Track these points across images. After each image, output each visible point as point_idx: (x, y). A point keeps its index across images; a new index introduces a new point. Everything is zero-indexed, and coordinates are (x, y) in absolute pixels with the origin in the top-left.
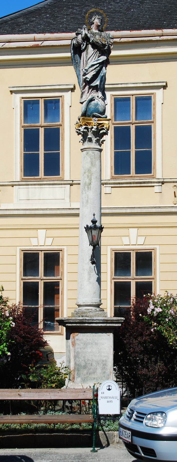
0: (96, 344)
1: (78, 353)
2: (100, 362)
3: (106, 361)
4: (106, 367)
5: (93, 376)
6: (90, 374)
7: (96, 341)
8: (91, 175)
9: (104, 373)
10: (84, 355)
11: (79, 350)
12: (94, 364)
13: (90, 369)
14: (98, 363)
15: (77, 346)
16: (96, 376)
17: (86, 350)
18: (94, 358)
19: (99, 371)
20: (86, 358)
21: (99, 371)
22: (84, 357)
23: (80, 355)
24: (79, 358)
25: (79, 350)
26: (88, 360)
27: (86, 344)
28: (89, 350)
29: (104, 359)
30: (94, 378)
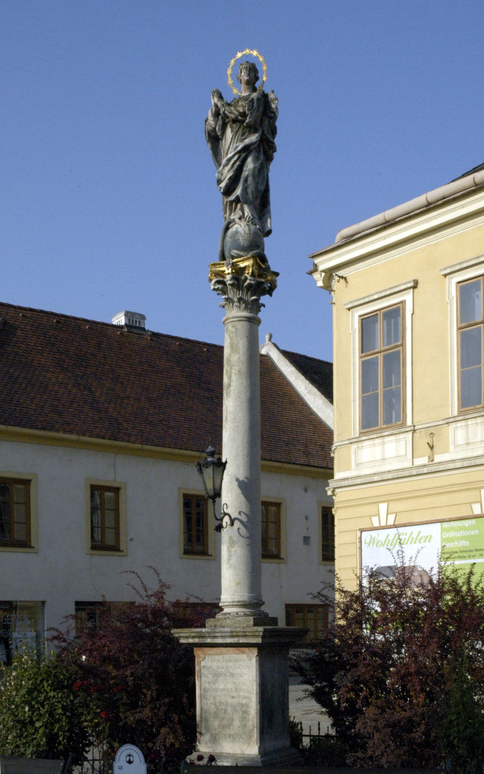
0: (232, 675)
1: (206, 690)
2: (238, 708)
3: (247, 705)
4: (247, 717)
6: (223, 727)
7: (231, 670)
8: (231, 368)
9: (245, 726)
11: (207, 685)
12: (229, 709)
13: (223, 719)
15: (204, 679)
17: (217, 685)
19: (237, 723)
20: (218, 700)
21: (237, 723)
22: (214, 698)
23: (209, 694)
24: (206, 699)
25: (207, 685)
26: (221, 703)
27: (216, 675)
28: (222, 686)
29: (244, 701)
30: (230, 736)
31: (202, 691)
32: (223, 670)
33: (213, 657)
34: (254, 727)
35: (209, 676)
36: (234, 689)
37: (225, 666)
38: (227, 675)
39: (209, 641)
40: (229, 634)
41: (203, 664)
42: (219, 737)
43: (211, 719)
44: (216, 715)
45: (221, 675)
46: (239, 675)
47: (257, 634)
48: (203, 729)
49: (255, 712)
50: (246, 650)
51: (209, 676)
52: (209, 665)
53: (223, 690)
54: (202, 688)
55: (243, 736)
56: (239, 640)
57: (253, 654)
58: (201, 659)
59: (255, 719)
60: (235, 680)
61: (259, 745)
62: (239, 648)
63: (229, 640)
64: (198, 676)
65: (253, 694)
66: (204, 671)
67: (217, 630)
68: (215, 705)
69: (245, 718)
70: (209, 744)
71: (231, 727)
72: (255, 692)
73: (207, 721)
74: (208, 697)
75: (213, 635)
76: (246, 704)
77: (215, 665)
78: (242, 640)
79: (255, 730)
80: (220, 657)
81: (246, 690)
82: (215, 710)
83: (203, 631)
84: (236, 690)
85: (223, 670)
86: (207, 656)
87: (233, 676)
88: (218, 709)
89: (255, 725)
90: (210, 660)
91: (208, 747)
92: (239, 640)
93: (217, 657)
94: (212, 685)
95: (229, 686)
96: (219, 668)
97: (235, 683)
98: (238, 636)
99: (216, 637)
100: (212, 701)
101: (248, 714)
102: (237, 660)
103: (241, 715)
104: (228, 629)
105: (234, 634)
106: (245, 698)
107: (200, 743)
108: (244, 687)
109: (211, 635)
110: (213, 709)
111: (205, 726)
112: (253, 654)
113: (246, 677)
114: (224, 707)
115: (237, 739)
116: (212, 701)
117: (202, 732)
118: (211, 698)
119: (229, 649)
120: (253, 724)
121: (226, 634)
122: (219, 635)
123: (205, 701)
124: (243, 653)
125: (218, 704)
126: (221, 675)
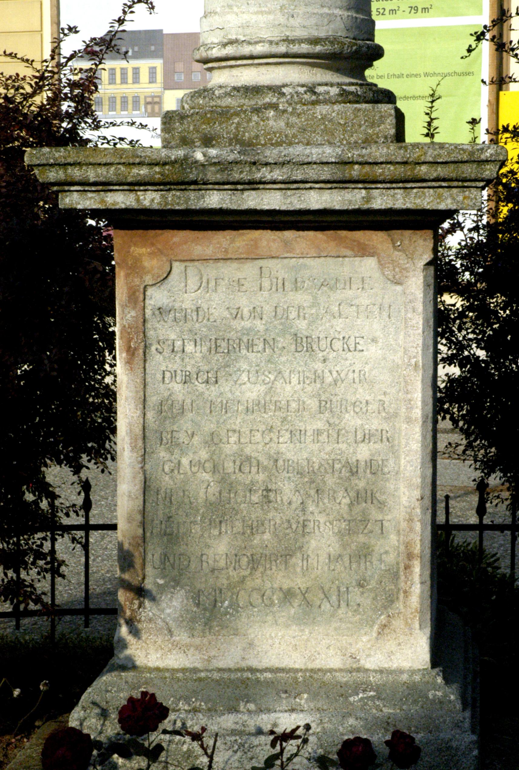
0: (304, 344)
1: (169, 410)
2: (330, 481)
3: (374, 468)
4: (375, 514)
5: (280, 579)
6: (254, 563)
7: (302, 325)
9: (364, 554)
10: (209, 426)
11: (177, 388)
12: (287, 489)
13: (253, 529)
14: (312, 481)
15: (158, 362)
16: (300, 582)
17: (225, 387)
18: (288, 450)
19: (323, 542)
20: (230, 447)
21: (323, 542)
22: (213, 440)
23: (186, 424)
24: (173, 445)
25: (177, 388)
26: (244, 461)
27: (226, 347)
28: (252, 392)
29: (363, 453)
30: (288, 595)
31: (150, 415)
32: (259, 325)
33: (211, 271)
34: (410, 556)
35: (190, 348)
36: (313, 404)
37: (268, 309)
38: (282, 342)
39: (214, 200)
40: (326, 173)
41: (157, 297)
42: (235, 605)
43: (196, 529)
44: (219, 512)
45: (250, 346)
46: (338, 345)
47: (469, 170)
48: (149, 570)
49: (417, 493)
50: (377, 238)
51: (190, 348)
52: (187, 301)
53: (260, 406)
54: (153, 400)
55: (355, 596)
56: (368, 199)
57: (411, 257)
58: (148, 279)
59: (418, 527)
60: (318, 366)
61: (428, 631)
62: (344, 233)
63: (316, 200)
64: (131, 352)
65: (409, 420)
66: (162, 330)
67: (272, 154)
68: (215, 469)
69: (365, 520)
70: (182, 637)
71: (297, 560)
72: (417, 413)
73: (171, 537)
74: (182, 437)
75: (245, 176)
76: (370, 463)
77: (217, 304)
78: (381, 200)
79: (417, 569)
80: (249, 270)
81: (373, 407)
82: (214, 489)
83: (199, 156)
84: (324, 406)
85: (259, 325)
86: (177, 267)
87: (310, 350)
88: (227, 484)
89: (417, 549)
90: (193, 282)
91: (176, 645)
92: (368, 199)
93: (229, 270)
94: (201, 387)
95: (288, 390)
96: (237, 315)
97: (317, 377)
98: (368, 182)
99: (253, 185)
100: (204, 455)
101: (382, 505)
102: (329, 284)
103: (345, 508)
104: (329, 153)
105: (356, 171)
106: (367, 437)
107: (135, 632)
108: (363, 394)
109: (236, 176)
110: (204, 486)
111: (165, 557)
112: (411, 257)
113: (373, 352)
114: (261, 477)
115: (326, 606)
116: (204, 455)
117: (148, 585)
118: (196, 440)
119: (289, 234)
120: (408, 545)
121: (312, 173)
122: (277, 174)
123: (163, 454)
124: (364, 251)
125: (230, 467)
126: (250, 346)
